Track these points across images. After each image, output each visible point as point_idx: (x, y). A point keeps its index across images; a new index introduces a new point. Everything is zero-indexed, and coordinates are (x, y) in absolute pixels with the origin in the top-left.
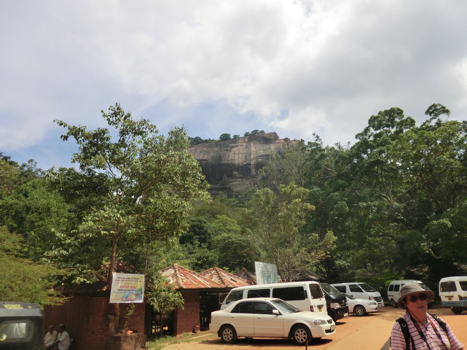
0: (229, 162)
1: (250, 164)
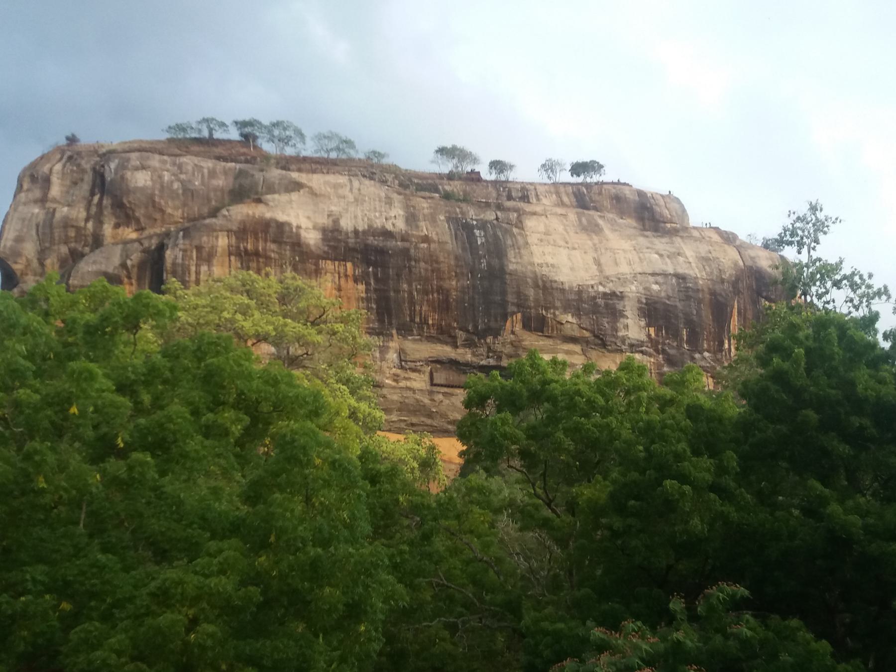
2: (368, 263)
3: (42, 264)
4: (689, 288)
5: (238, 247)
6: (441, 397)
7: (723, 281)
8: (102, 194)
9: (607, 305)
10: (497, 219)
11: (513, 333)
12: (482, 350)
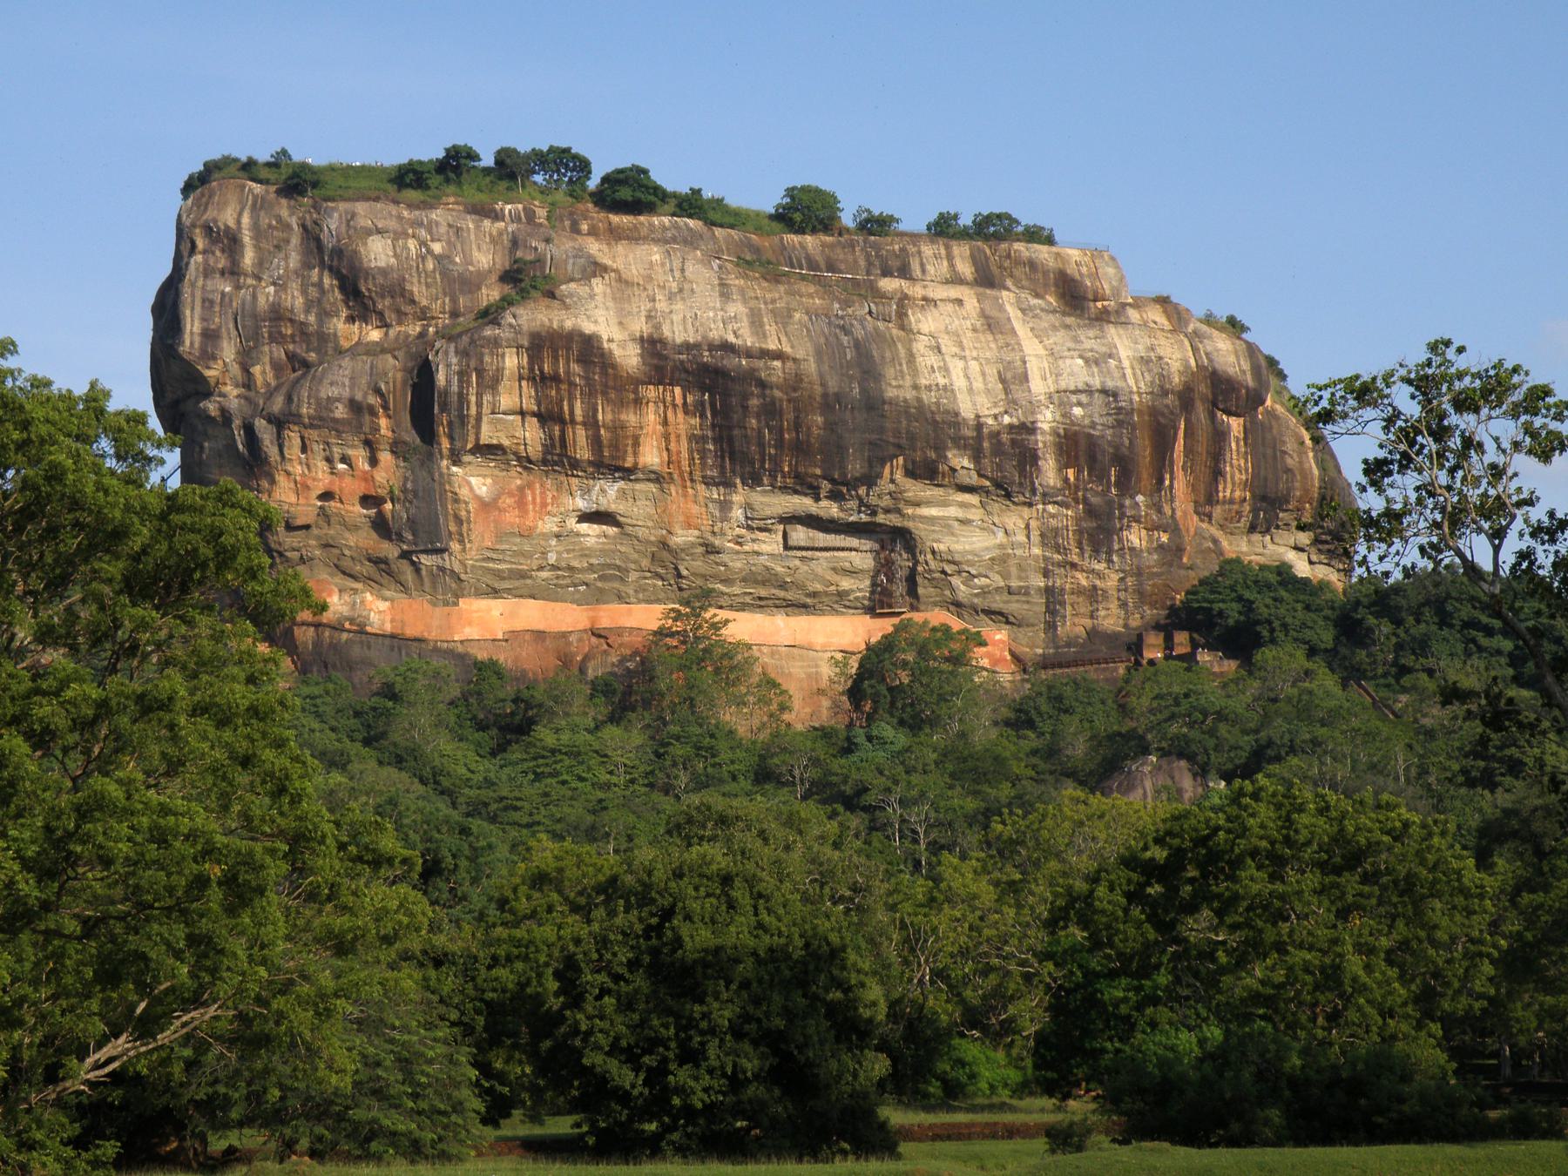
0: (929, 398)
1: (1028, 428)
2: (703, 389)
3: (246, 370)
4: (1120, 408)
5: (531, 370)
6: (797, 562)
7: (1165, 393)
8: (322, 265)
9: (1013, 442)
10: (870, 313)
11: (892, 481)
12: (853, 504)
